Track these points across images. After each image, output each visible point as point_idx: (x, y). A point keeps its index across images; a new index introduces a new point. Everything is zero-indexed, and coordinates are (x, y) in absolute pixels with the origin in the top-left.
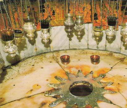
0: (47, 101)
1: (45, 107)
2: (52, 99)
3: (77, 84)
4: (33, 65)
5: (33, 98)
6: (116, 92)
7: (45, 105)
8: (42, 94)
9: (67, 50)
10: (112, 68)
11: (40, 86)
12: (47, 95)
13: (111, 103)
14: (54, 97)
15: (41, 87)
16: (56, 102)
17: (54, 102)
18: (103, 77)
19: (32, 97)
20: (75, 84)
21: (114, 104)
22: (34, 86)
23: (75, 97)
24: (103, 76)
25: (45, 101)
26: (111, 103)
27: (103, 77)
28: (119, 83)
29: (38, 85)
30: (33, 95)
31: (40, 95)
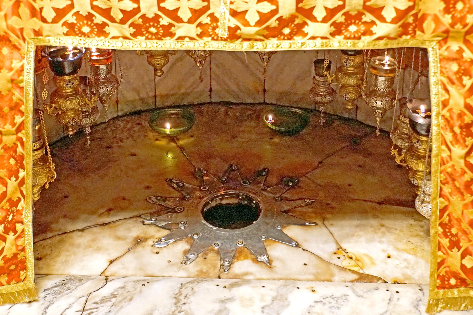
0: (148, 236)
1: (143, 247)
2: (159, 231)
3: (221, 199)
4: (108, 147)
5: (116, 226)
6: (316, 224)
7: (144, 244)
8: (135, 219)
9: (204, 104)
10: (320, 163)
11: (130, 201)
12: (147, 222)
13: (297, 246)
14: (164, 228)
15: (131, 203)
16: (167, 238)
17: (163, 237)
18: (293, 187)
19: (111, 225)
20: (218, 202)
21: (304, 250)
22: (115, 200)
23: (215, 228)
24: (291, 184)
25: (142, 235)
26: (297, 246)
27: (293, 187)
28: (329, 202)
29: (124, 199)
30: (114, 222)
31: (131, 221)
